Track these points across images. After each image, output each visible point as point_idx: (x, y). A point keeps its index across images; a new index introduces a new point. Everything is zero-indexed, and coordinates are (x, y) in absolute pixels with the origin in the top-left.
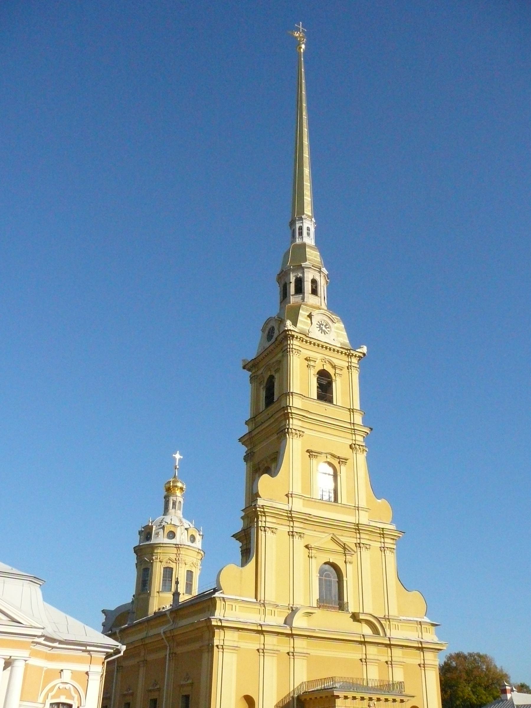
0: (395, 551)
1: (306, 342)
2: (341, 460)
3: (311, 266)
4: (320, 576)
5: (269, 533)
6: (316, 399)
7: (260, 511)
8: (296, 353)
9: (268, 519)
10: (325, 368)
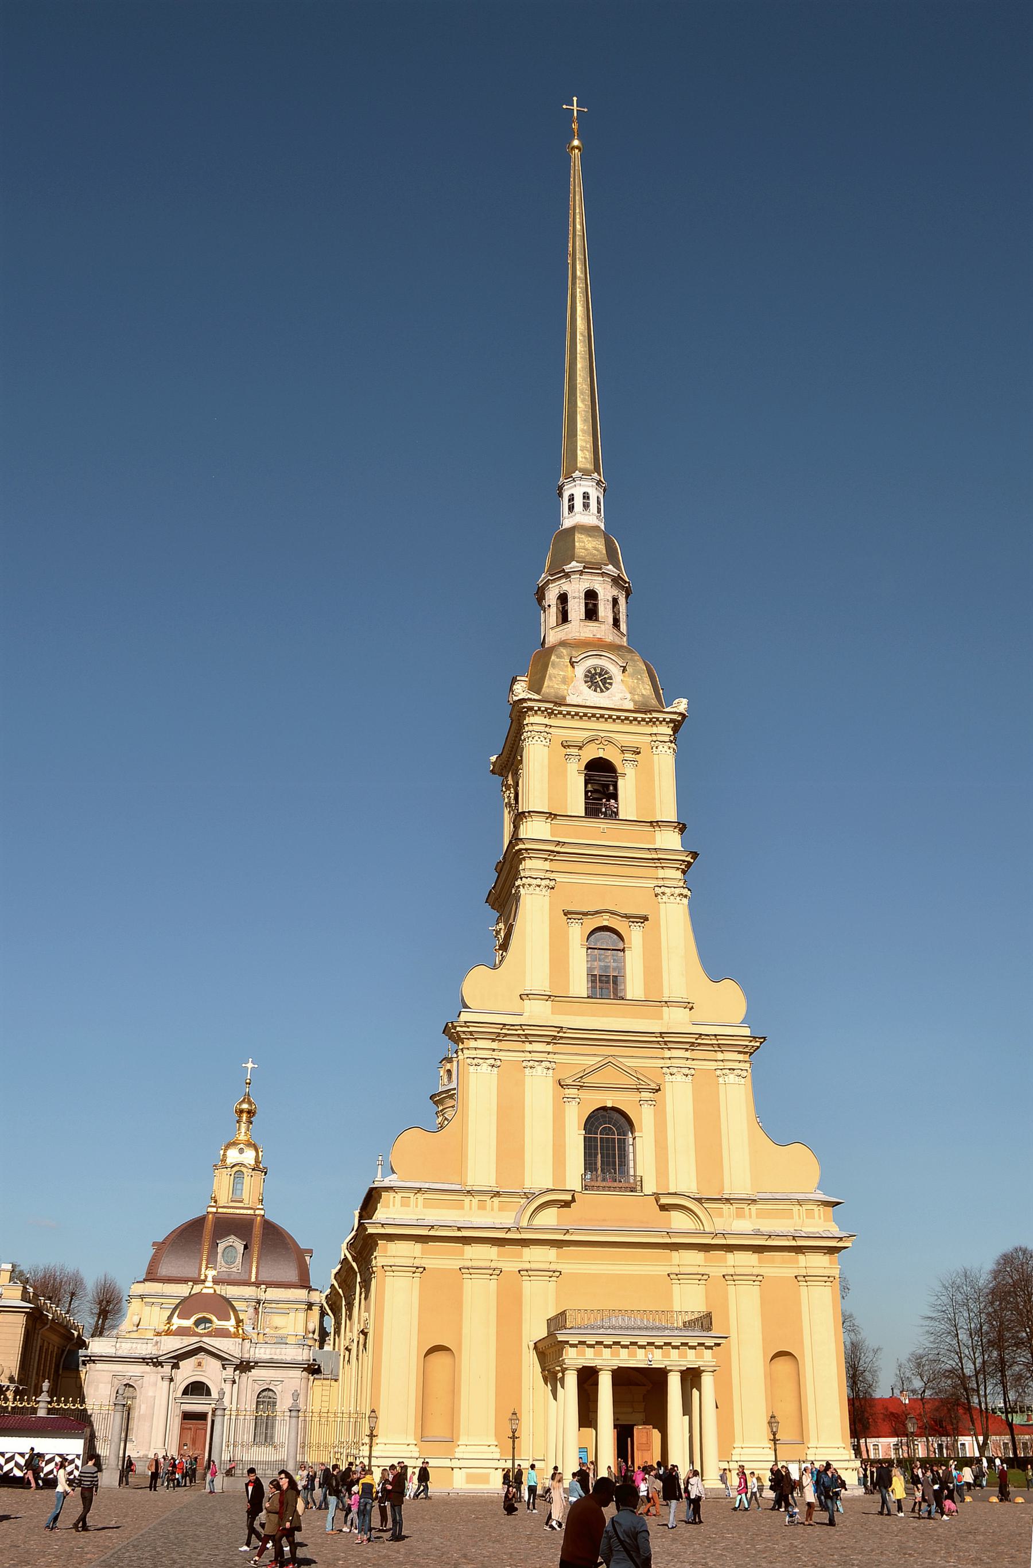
0: (748, 1074)
1: (560, 713)
2: (631, 920)
3: (582, 569)
4: (586, 1134)
5: (485, 1067)
6: (584, 815)
8: (542, 739)
9: (480, 1044)
10: (601, 754)
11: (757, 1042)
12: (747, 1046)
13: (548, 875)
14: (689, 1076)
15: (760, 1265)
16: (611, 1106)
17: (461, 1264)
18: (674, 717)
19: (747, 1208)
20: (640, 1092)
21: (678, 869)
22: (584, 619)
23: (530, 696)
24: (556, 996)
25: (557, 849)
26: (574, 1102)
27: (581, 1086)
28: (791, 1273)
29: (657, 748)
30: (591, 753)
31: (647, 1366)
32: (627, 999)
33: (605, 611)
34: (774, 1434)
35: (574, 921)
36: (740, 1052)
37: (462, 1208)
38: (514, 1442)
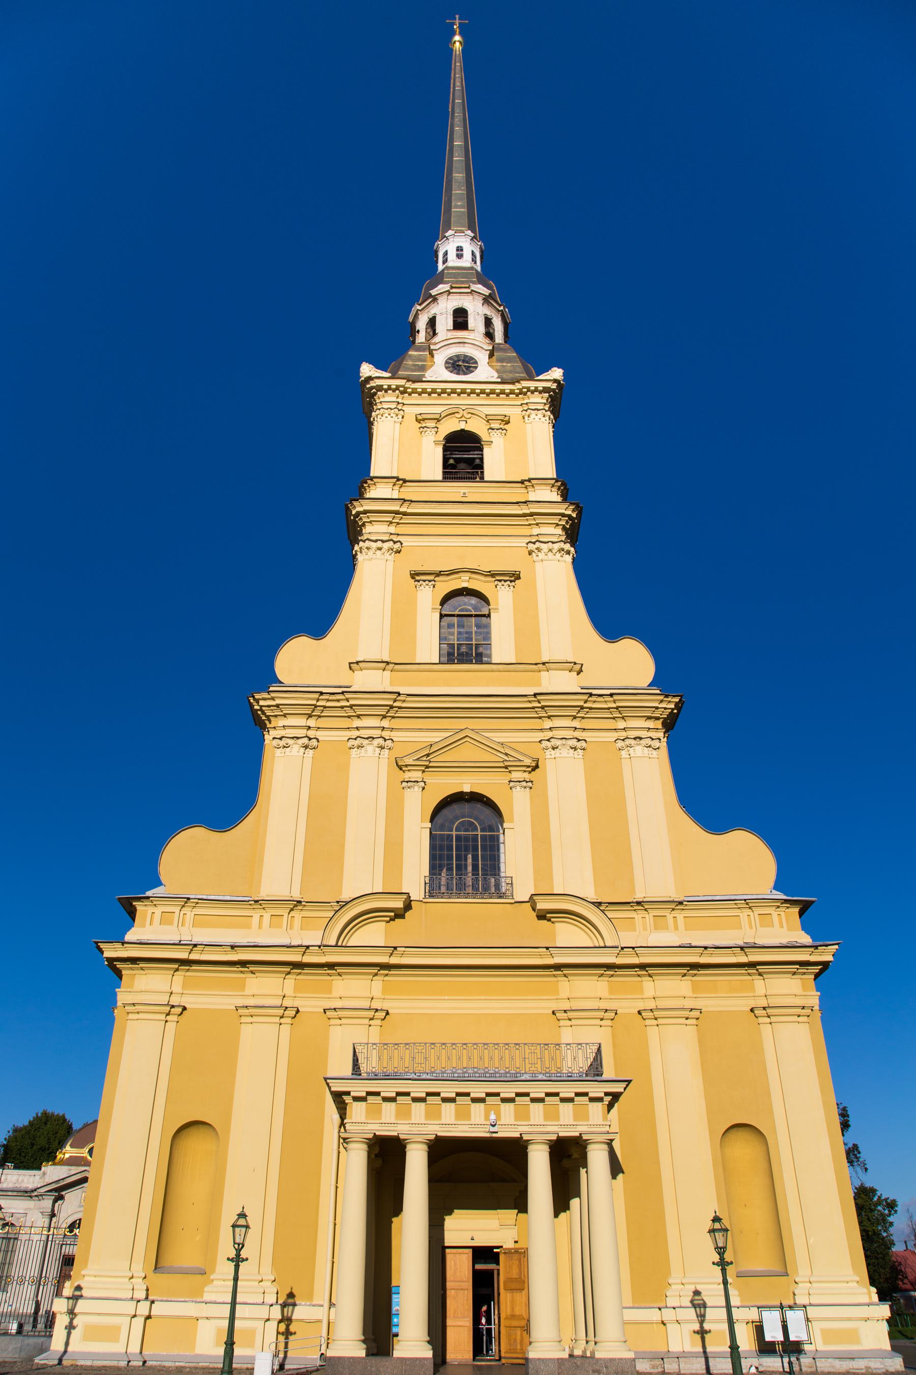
1: (414, 391)
7: (269, 706)
10: (462, 426)
11: (670, 702)
12: (657, 708)
13: (395, 538)
14: (579, 750)
15: (695, 996)
16: (469, 791)
17: (241, 1002)
18: (548, 385)
19: (670, 917)
20: (510, 772)
21: (557, 525)
22: (452, 329)
23: (377, 375)
24: (396, 664)
25: (403, 509)
26: (416, 788)
27: (427, 767)
28: (744, 1005)
29: (529, 417)
30: (451, 426)
31: (488, 1135)
32: (493, 662)
33: (476, 323)
34: (721, 1251)
35: (424, 583)
36: (649, 718)
37: (248, 927)
38: (237, 1267)
